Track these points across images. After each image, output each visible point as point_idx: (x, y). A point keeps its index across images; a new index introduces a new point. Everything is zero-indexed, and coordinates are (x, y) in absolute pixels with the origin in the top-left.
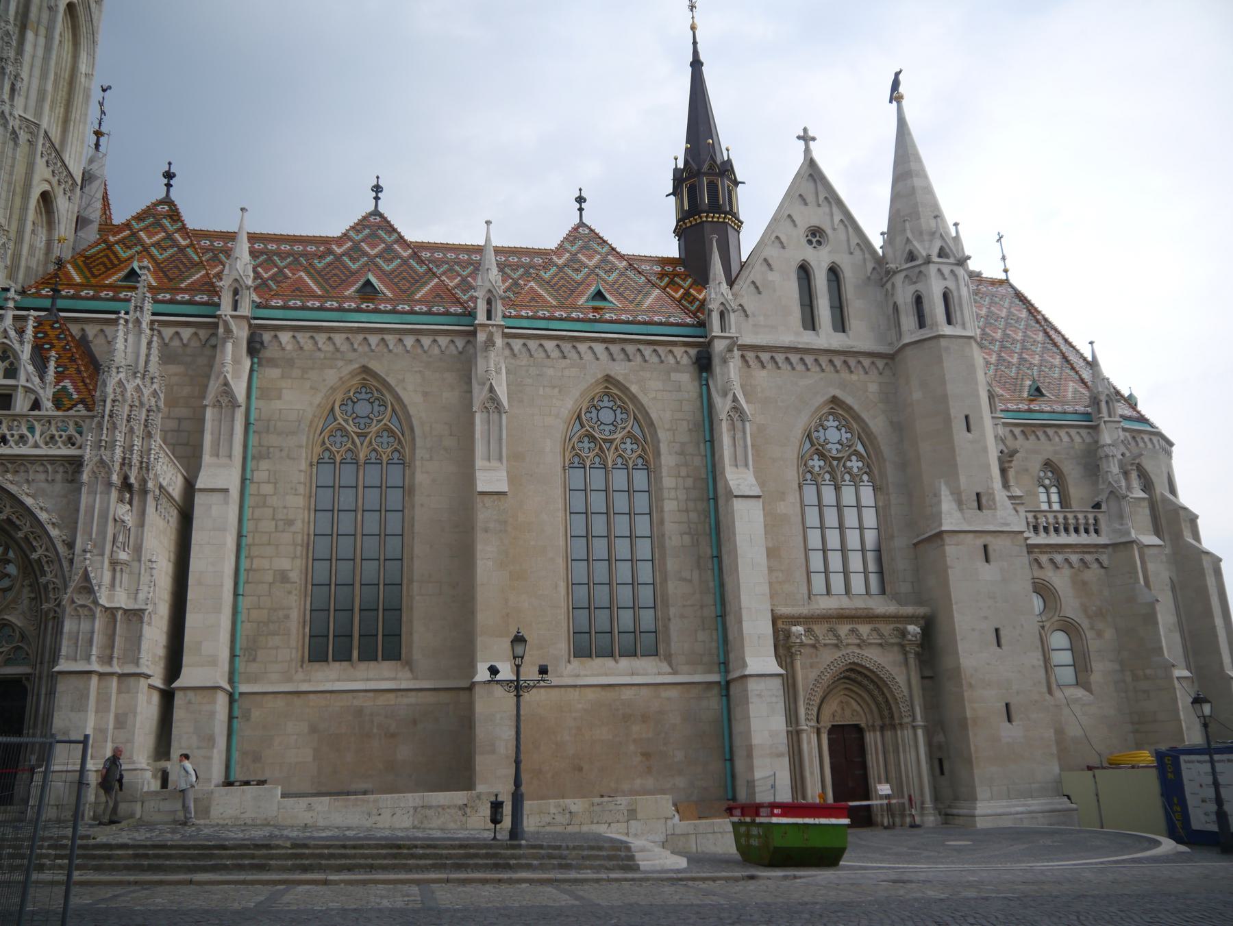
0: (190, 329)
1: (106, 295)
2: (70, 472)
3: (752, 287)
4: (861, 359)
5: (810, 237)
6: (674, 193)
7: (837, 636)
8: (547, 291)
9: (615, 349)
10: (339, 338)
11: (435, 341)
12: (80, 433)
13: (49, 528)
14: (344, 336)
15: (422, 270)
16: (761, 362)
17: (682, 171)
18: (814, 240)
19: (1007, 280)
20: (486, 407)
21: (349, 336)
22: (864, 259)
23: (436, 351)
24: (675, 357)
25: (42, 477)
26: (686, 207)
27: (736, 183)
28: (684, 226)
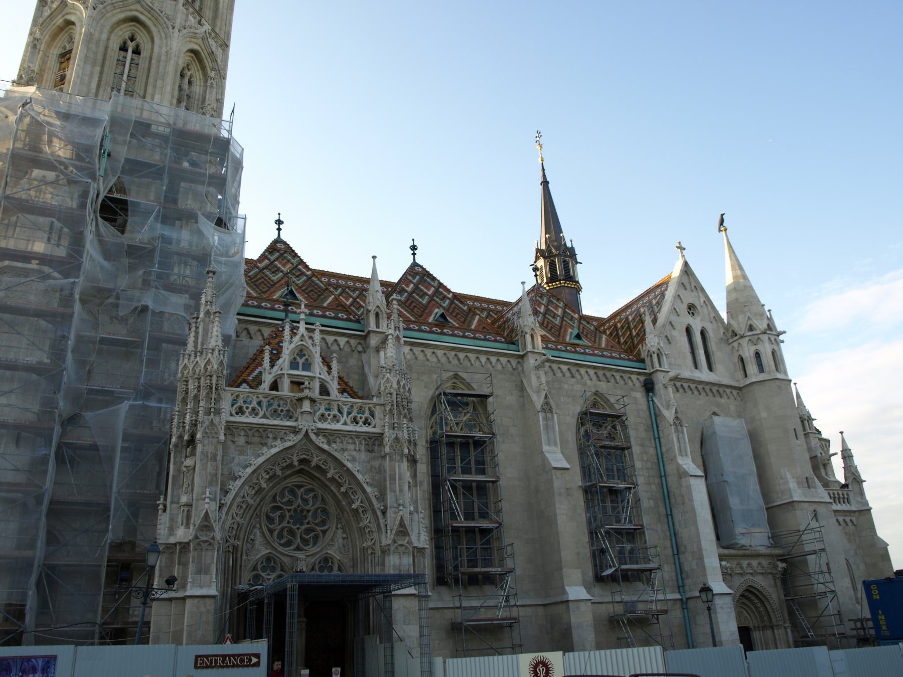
0: (344, 338)
1: (329, 314)
2: (371, 445)
4: (726, 390)
7: (742, 568)
9: (600, 373)
10: (440, 353)
11: (498, 360)
12: (373, 416)
13: (365, 485)
14: (443, 352)
15: (465, 308)
16: (677, 388)
18: (691, 312)
20: (544, 409)
21: (446, 352)
22: (718, 327)
23: (499, 367)
25: (352, 447)
27: (577, 263)
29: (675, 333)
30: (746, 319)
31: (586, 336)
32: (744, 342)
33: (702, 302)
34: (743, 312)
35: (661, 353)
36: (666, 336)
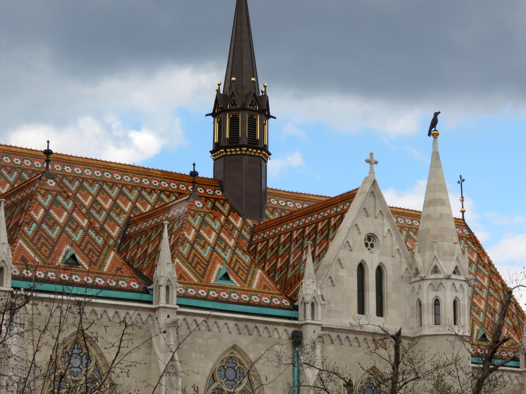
3: (329, 280)
5: (367, 241)
6: (214, 115)
8: (189, 269)
9: (241, 325)
16: (331, 339)
17: (224, 95)
18: (369, 243)
19: (463, 219)
22: (401, 262)
24: (278, 333)
26: (227, 136)
27: (269, 116)
28: (225, 154)
29: (342, 273)
30: (432, 259)
31: (237, 273)
32: (425, 284)
33: (386, 229)
34: (432, 248)
35: (316, 302)
36: (330, 277)
